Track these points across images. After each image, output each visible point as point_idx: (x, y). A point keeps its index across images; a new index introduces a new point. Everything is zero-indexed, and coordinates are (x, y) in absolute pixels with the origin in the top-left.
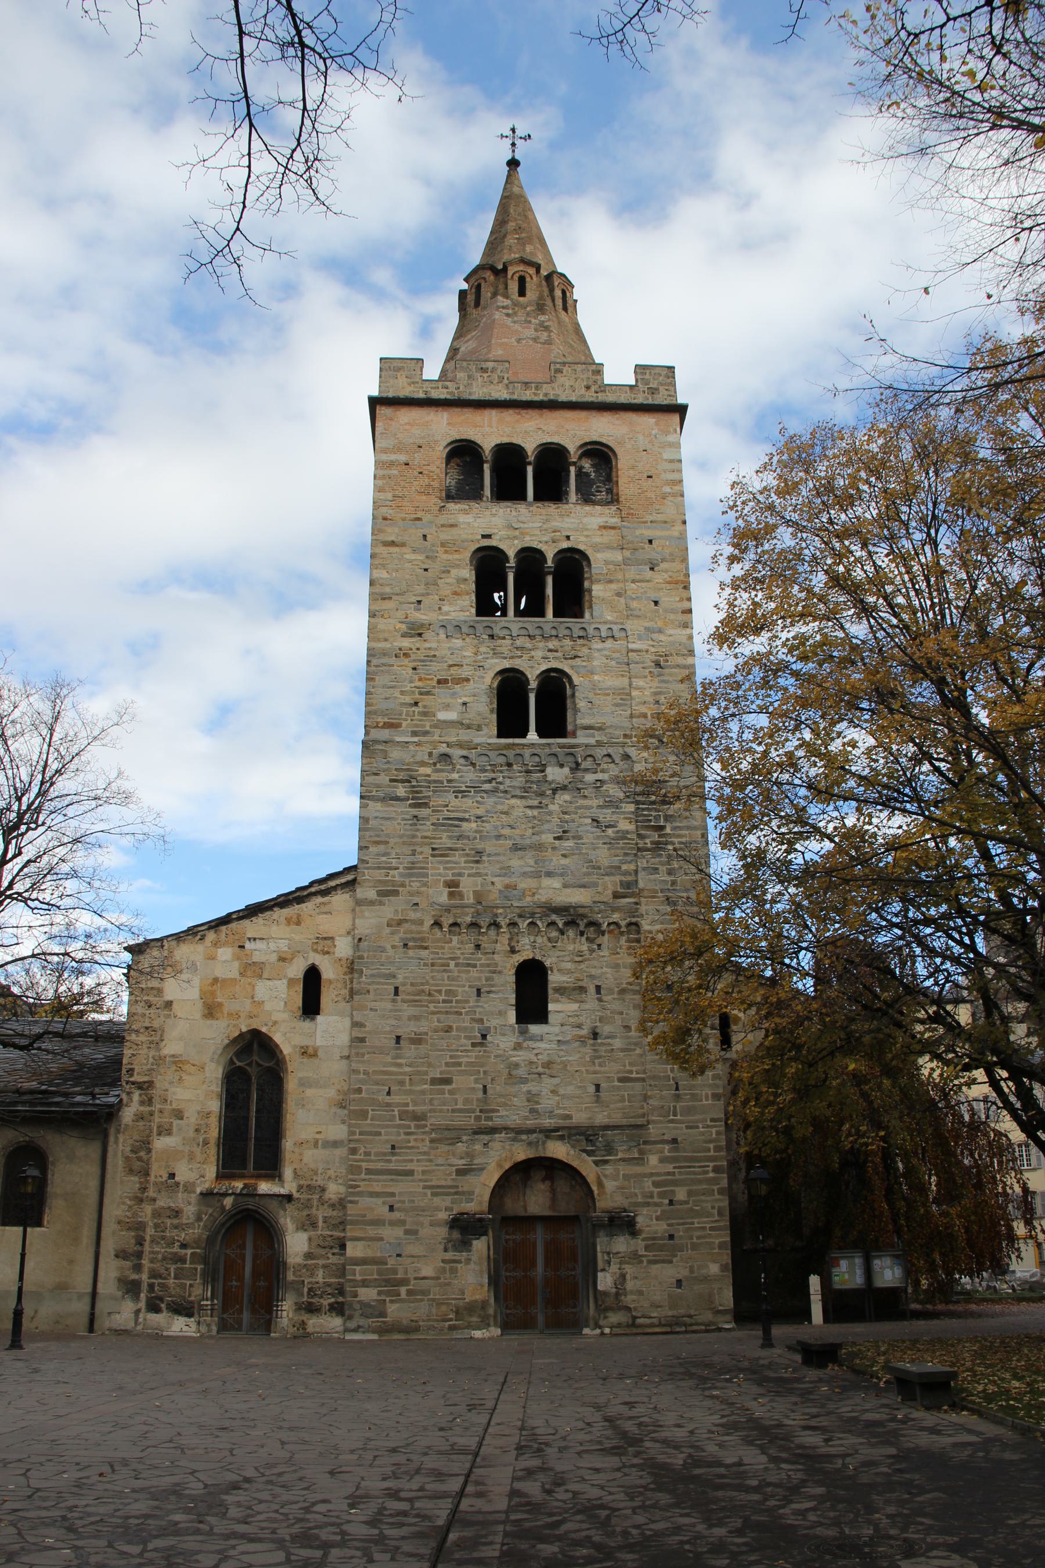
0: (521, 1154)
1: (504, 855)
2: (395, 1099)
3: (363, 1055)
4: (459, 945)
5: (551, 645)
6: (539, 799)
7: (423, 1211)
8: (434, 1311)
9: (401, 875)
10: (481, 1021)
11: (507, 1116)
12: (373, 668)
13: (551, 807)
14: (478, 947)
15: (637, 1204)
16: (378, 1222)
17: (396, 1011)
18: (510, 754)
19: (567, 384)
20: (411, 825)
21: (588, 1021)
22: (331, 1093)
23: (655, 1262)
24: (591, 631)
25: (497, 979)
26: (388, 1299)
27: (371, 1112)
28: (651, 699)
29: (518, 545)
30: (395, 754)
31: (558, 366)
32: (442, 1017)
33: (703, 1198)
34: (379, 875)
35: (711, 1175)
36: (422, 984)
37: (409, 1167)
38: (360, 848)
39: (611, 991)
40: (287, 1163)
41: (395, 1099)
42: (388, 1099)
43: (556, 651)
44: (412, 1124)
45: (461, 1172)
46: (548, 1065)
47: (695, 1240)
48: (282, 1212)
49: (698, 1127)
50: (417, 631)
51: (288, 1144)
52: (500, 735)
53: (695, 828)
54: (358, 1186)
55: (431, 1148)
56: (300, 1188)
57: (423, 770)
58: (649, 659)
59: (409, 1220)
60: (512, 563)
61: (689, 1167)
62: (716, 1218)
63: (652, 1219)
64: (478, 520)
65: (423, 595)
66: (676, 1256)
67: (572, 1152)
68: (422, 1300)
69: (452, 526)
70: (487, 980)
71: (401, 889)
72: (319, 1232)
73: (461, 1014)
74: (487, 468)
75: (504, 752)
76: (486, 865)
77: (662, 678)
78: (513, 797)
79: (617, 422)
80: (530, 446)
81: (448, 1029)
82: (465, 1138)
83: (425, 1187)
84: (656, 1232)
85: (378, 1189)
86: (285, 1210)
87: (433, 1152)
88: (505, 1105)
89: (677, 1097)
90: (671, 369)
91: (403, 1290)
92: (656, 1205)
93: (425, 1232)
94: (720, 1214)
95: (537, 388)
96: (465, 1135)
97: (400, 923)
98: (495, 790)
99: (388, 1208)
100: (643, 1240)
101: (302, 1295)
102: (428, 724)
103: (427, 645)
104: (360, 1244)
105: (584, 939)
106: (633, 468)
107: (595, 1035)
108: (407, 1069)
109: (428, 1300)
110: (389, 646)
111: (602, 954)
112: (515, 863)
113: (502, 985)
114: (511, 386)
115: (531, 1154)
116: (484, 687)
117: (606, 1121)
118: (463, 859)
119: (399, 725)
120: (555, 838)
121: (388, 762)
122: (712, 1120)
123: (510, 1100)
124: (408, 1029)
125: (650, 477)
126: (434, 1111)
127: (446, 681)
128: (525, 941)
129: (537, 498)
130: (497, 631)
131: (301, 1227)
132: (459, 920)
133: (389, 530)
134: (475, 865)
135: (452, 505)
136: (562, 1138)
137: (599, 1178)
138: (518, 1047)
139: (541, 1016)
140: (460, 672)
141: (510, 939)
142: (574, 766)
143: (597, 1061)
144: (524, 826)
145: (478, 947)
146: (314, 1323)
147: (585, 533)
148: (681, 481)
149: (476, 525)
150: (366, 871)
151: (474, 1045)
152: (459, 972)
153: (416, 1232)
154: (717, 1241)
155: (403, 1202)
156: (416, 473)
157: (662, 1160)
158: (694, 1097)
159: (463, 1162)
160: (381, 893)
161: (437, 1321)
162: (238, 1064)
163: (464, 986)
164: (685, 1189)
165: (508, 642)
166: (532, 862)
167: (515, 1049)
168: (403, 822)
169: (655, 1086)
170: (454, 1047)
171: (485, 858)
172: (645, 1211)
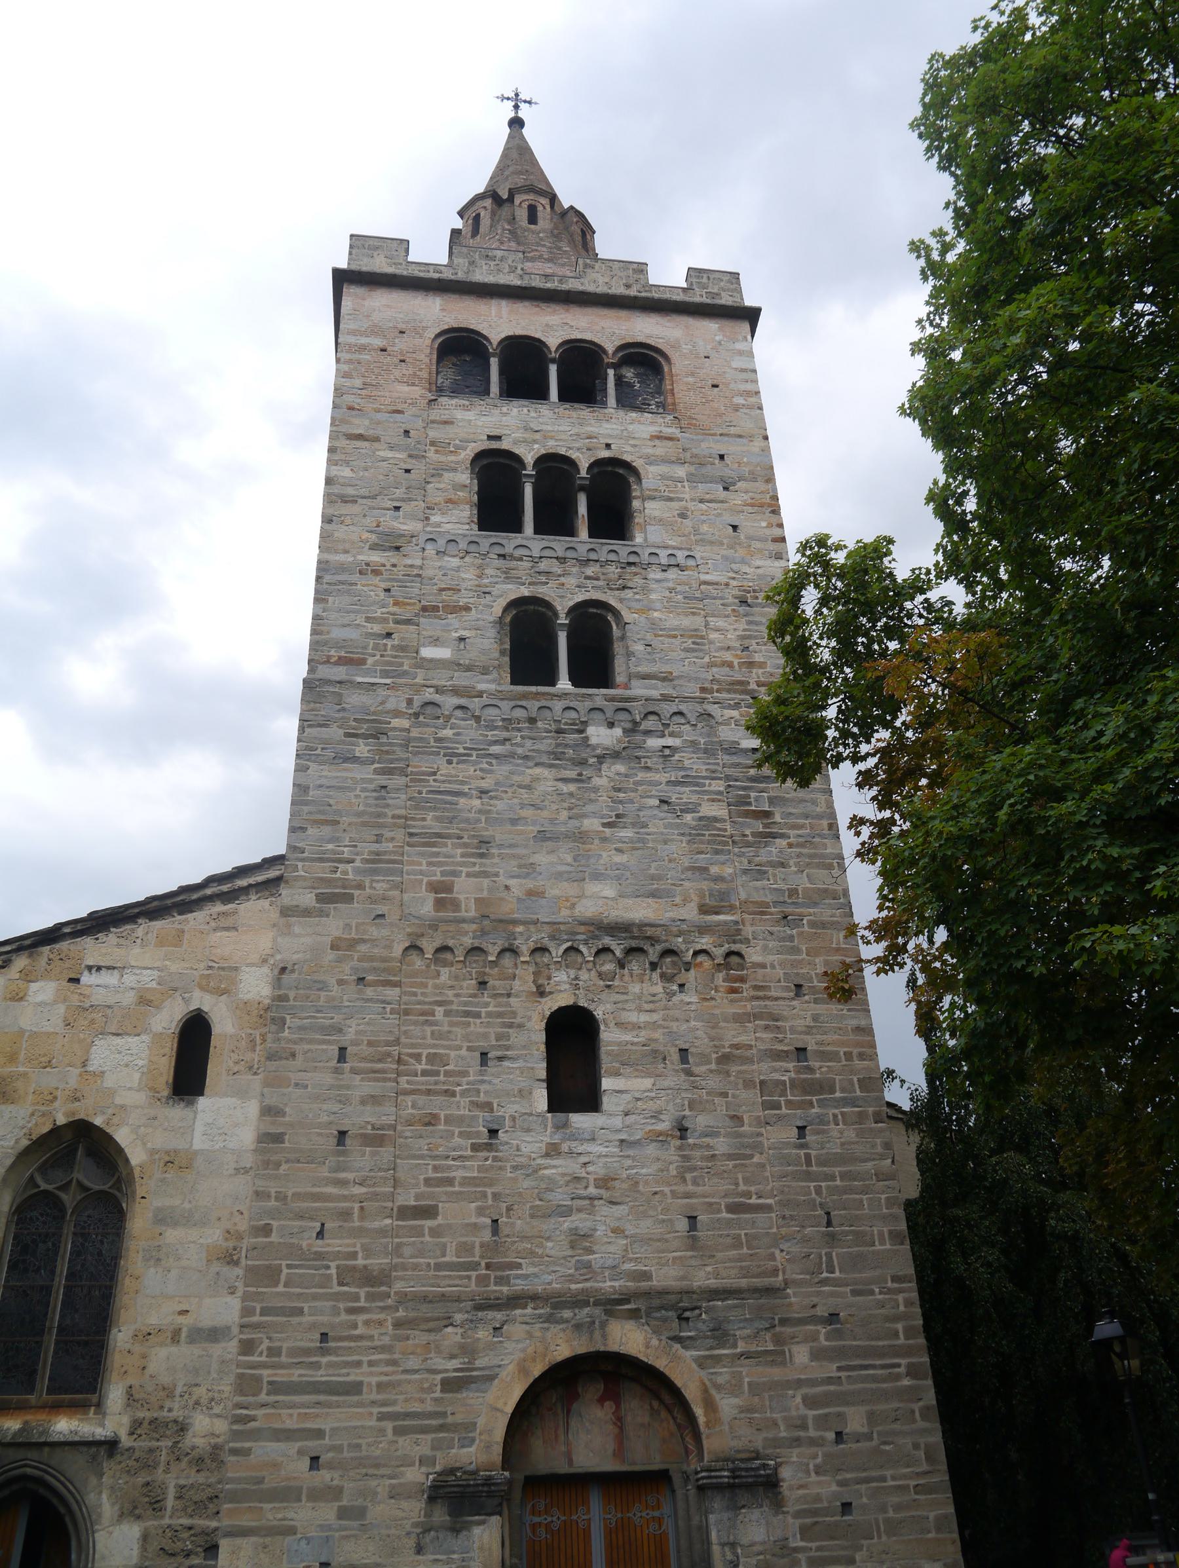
0: (563, 1347)
1: (526, 847)
2: (333, 1244)
3: (278, 1165)
5: (589, 571)
6: (578, 770)
7: (377, 1466)
9: (357, 871)
10: (488, 1106)
11: (536, 1275)
12: (325, 586)
13: (597, 781)
14: (483, 984)
15: (776, 1443)
16: (288, 1494)
17: (340, 1087)
18: (533, 705)
19: (601, 280)
20: (377, 799)
21: (670, 1107)
22: (214, 1236)
24: (645, 557)
25: (516, 1038)
27: (285, 1271)
28: (737, 645)
29: (539, 450)
30: (355, 699)
32: (421, 1100)
33: (897, 1426)
34: (321, 870)
37: (354, 1376)
38: (293, 830)
39: (704, 1059)
40: (114, 1376)
41: (333, 1244)
42: (319, 1246)
43: (597, 579)
44: (362, 1293)
45: (452, 1385)
46: (604, 1182)
47: (891, 1514)
48: (93, 1481)
49: (872, 1293)
50: (393, 543)
51: (121, 1337)
52: (513, 682)
53: (820, 817)
54: (253, 1419)
55: (396, 1338)
56: (136, 1425)
57: (396, 722)
58: (730, 595)
59: (348, 1486)
62: (925, 1467)
63: (808, 1472)
64: (484, 418)
65: (403, 500)
66: (860, 1548)
69: (446, 422)
71: (356, 893)
72: (167, 1521)
73: (453, 1094)
74: (494, 363)
75: (523, 703)
76: (496, 860)
77: (751, 618)
78: (537, 765)
80: (553, 341)
81: (431, 1121)
83: (382, 1417)
84: (818, 1498)
85: (290, 1424)
86: (102, 1475)
87: (399, 1346)
89: (832, 1239)
90: (735, 276)
92: (813, 1442)
93: (380, 1511)
94: (929, 1458)
96: (460, 1311)
97: (353, 944)
98: (512, 755)
99: (307, 1462)
100: (798, 1514)
103: (409, 562)
105: (656, 976)
106: (692, 374)
107: (682, 1130)
108: (358, 1190)
111: (687, 999)
112: (542, 859)
113: (524, 1047)
115: (581, 1346)
116: (492, 619)
117: (712, 1283)
118: (459, 851)
119: (363, 662)
120: (605, 825)
121: (344, 709)
122: (895, 1279)
123: (541, 1246)
124: (359, 1118)
126: (404, 1267)
127: (435, 609)
128: (561, 977)
129: (564, 397)
130: (509, 549)
131: (130, 1512)
132: (451, 943)
133: (356, 421)
134: (478, 861)
136: (634, 1315)
137: (706, 1391)
138: (553, 1151)
139: (590, 1101)
140: (455, 598)
141: (536, 974)
142: (628, 726)
143: (688, 1176)
144: (554, 807)
145: (483, 984)
147: (632, 442)
148: (758, 393)
150: (300, 864)
151: (475, 1148)
152: (451, 1024)
153: (360, 1513)
154: (932, 1515)
155: (338, 1449)
156: (396, 360)
157: (818, 1355)
158: (861, 1238)
159: (455, 1364)
160: (321, 898)
162: (44, 1186)
163: (460, 1048)
164: (863, 1409)
165: (526, 564)
166: (569, 859)
167: (547, 1155)
168: (363, 795)
169: (792, 1218)
170: (441, 1151)
171: (494, 851)
172: (794, 1455)
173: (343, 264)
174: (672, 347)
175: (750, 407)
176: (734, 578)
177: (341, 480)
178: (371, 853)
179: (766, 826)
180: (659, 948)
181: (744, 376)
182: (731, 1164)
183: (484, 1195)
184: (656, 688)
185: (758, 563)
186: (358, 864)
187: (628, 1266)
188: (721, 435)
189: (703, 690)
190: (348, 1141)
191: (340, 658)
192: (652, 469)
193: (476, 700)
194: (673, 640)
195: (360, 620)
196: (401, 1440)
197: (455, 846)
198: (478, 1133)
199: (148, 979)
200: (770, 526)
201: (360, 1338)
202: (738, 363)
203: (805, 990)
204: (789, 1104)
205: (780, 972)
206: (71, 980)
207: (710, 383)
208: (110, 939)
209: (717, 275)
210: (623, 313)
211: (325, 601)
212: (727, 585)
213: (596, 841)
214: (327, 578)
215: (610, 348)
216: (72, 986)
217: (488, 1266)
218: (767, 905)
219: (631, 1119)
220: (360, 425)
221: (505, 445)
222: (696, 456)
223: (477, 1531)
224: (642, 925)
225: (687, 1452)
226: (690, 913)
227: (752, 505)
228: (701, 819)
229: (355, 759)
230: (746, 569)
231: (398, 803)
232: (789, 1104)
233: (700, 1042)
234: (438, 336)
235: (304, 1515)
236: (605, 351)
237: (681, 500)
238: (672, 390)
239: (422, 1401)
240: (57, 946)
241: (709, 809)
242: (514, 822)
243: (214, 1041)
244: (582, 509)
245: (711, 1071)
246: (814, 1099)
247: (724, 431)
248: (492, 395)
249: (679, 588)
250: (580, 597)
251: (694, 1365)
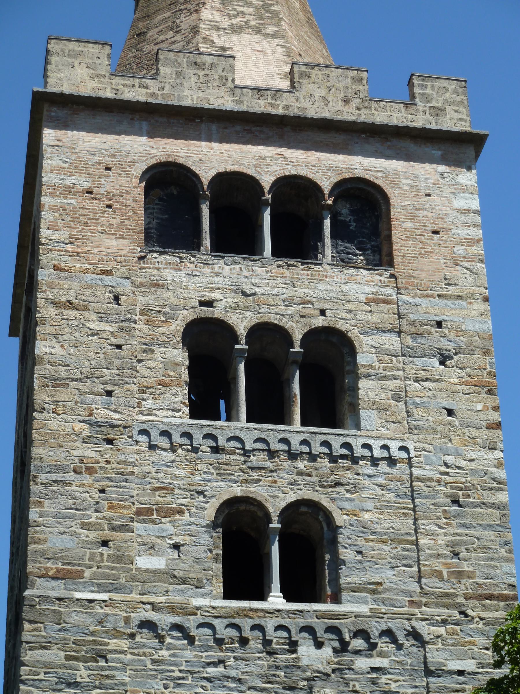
19: (318, 93)
31: (303, 68)
57: (114, 643)
69: (156, 286)
75: (237, 621)
95: (274, 98)
106: (412, 218)
114: (238, 91)
119: (80, 575)
121: (64, 629)
127: (149, 512)
129: (277, 253)
133: (64, 284)
149: (191, 286)
176: (447, 474)
184: (366, 603)
185: (472, 455)
188: (439, 296)
191: (58, 570)
192: (366, 339)
193: (192, 617)
194: (384, 547)
212: (439, 481)
215: (326, 186)
221: (217, 312)
222: (413, 323)
234: (145, 172)
247: (443, 292)
249: (392, 485)
250: (292, 497)
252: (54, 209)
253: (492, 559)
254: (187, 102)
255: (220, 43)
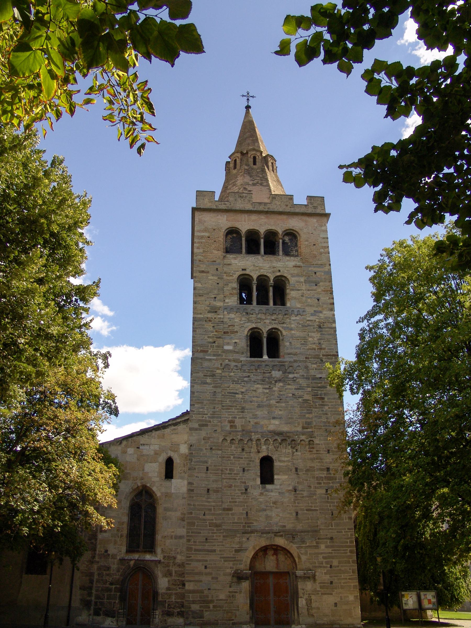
0: (263, 542)
1: (254, 409)
2: (207, 517)
3: (193, 497)
4: (234, 449)
8: (225, 615)
10: (245, 483)
15: (315, 567)
16: (200, 573)
17: (207, 477)
22: (178, 514)
23: (325, 594)
26: (204, 610)
27: (196, 523)
30: (206, 364)
32: (228, 481)
34: (199, 417)
35: (349, 554)
36: (219, 466)
37: (214, 548)
41: (207, 517)
42: (204, 517)
43: (275, 320)
44: (215, 529)
45: (237, 551)
46: (275, 503)
47: (342, 584)
48: (156, 568)
49: (342, 532)
50: (214, 310)
51: (159, 537)
54: (191, 557)
56: (164, 557)
57: (218, 371)
60: (255, 282)
61: (339, 550)
62: (351, 574)
64: (241, 262)
65: (217, 295)
66: (334, 591)
67: (286, 542)
68: (220, 610)
70: (248, 464)
71: (209, 424)
72: (173, 578)
73: (236, 479)
74: (244, 239)
75: (254, 364)
76: (246, 414)
78: (258, 384)
79: (300, 221)
80: (262, 231)
81: (230, 486)
82: (238, 535)
83: (221, 558)
85: (199, 558)
86: (158, 567)
88: (256, 520)
91: (211, 606)
92: (324, 567)
94: (353, 572)
97: (209, 438)
101: (165, 607)
102: (220, 351)
103: (219, 316)
104: (192, 583)
105: (290, 447)
106: (307, 241)
107: (295, 490)
108: (213, 504)
109: (223, 610)
110: (202, 316)
112: (259, 413)
116: (244, 335)
118: (236, 411)
119: (207, 351)
121: (203, 368)
122: (348, 529)
125: (314, 245)
127: (228, 332)
128: (264, 447)
129: (265, 253)
130: (249, 311)
131: (165, 576)
132: (234, 438)
133: (202, 266)
135: (229, 255)
136: (281, 536)
137: (298, 555)
138: (261, 494)
139: (271, 481)
143: (296, 502)
144: (262, 397)
145: (243, 450)
146: (171, 620)
150: (194, 415)
151: (242, 493)
152: (235, 461)
156: (213, 241)
157: (327, 547)
160: (200, 425)
161: (227, 620)
165: (254, 316)
166: (266, 413)
167: (260, 495)
169: (323, 513)
172: (319, 570)
173: (195, 206)
174: (301, 230)
175: (325, 253)
177: (198, 288)
178: (212, 412)
179: (323, 402)
180: (291, 439)
181: (324, 240)
182: (307, 498)
183: (244, 505)
186: (209, 415)
187: (280, 524)
189: (306, 358)
190: (210, 491)
192: (293, 279)
195: (206, 338)
196: (226, 563)
197: (235, 409)
198: (242, 490)
199: (157, 447)
200: (329, 298)
201: (215, 539)
202: (322, 236)
203: (330, 451)
204: (324, 483)
205: (324, 446)
206: (137, 448)
207: (313, 244)
208: (146, 436)
209: (317, 199)
210: (285, 217)
211: (196, 331)
212: (315, 321)
213: (274, 407)
214: (196, 323)
216: (138, 449)
217: (245, 523)
218: (321, 427)
219: (282, 486)
220: (203, 267)
221: (247, 272)
223: (243, 583)
224: (287, 432)
225: (294, 568)
226: (299, 429)
227: (324, 291)
228: (304, 400)
229: (206, 383)
230: (321, 315)
231: (219, 397)
232: (324, 483)
233: (301, 465)
234: (225, 230)
235: (204, 578)
236: (279, 233)
237: (301, 290)
238: (300, 247)
239: (230, 554)
240: (133, 438)
241: (306, 397)
242: (251, 402)
243: (174, 465)
244: (271, 294)
245: (304, 474)
246: (331, 482)
248: (243, 253)
250: (270, 327)
251: (296, 548)
252: (199, 243)
253: (330, 344)
254: (238, 208)
255: (249, 189)
